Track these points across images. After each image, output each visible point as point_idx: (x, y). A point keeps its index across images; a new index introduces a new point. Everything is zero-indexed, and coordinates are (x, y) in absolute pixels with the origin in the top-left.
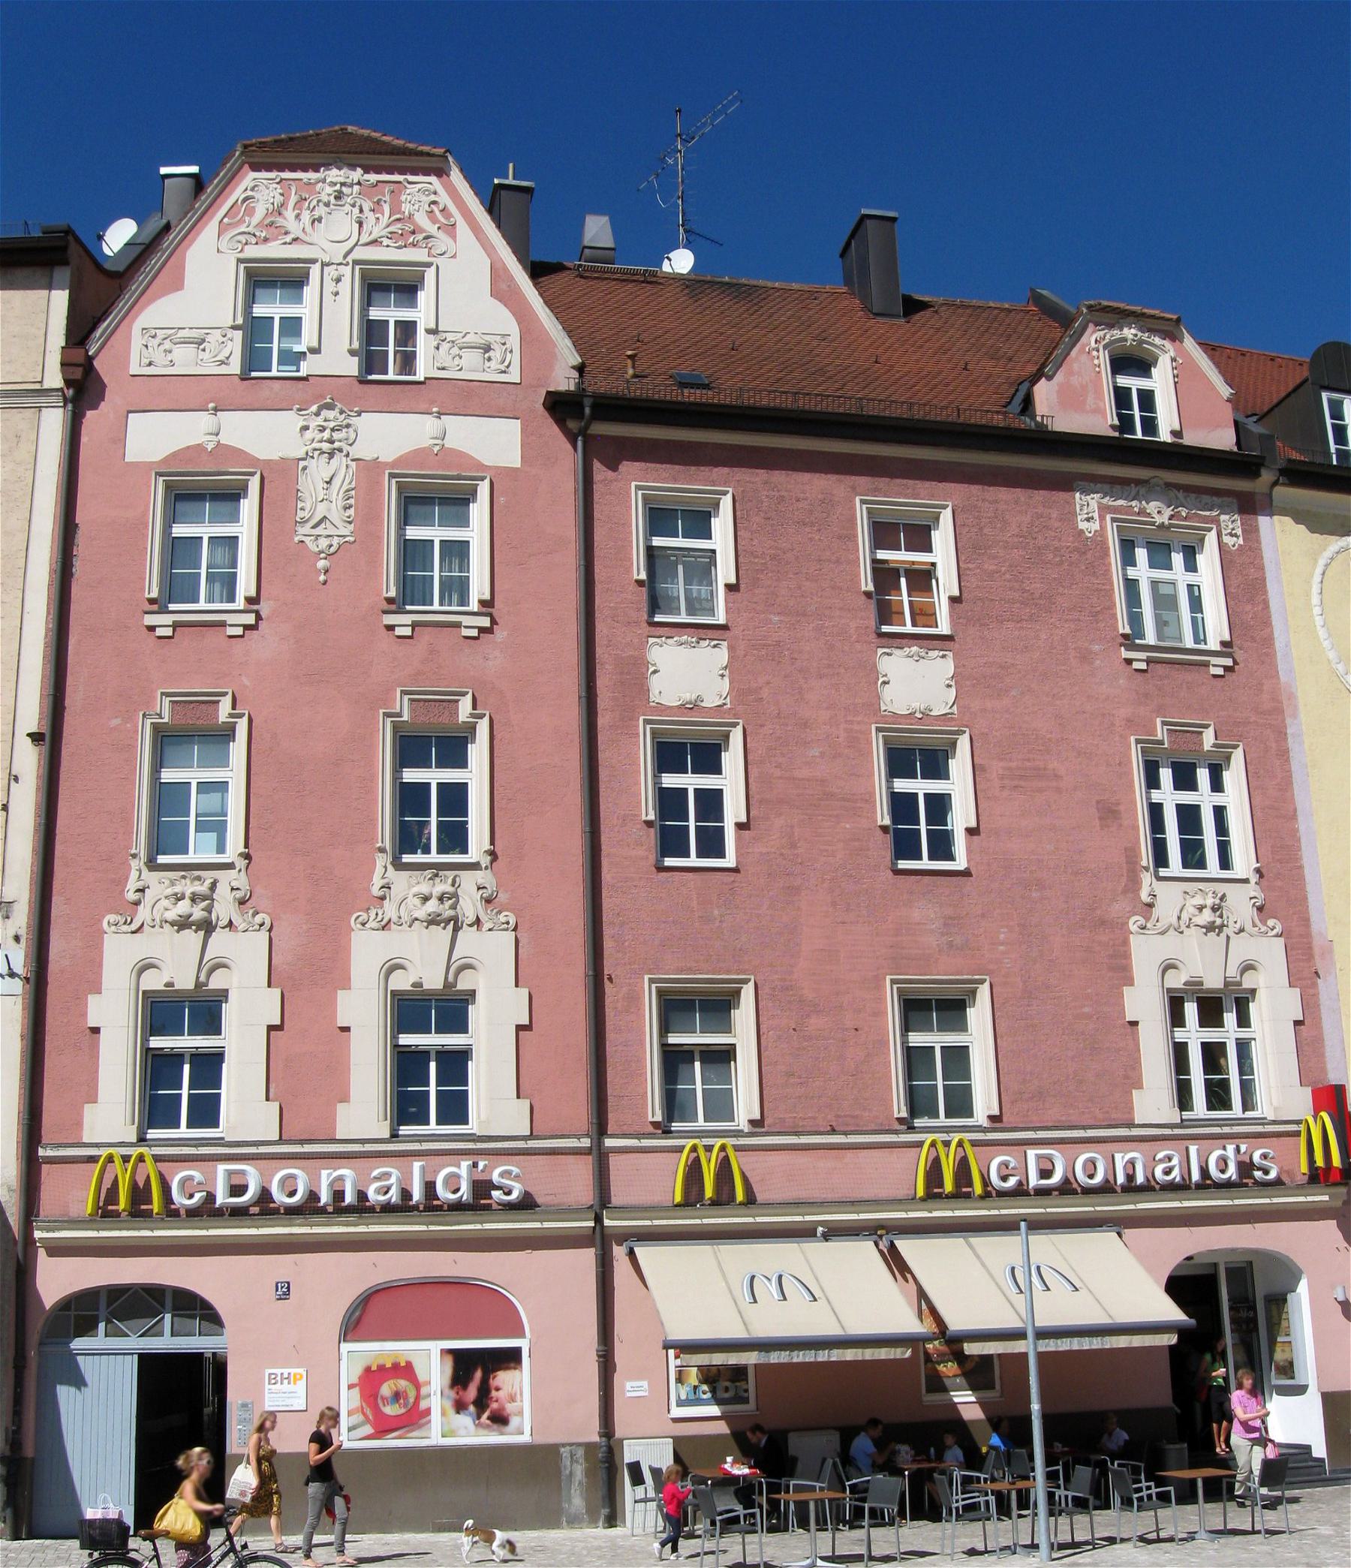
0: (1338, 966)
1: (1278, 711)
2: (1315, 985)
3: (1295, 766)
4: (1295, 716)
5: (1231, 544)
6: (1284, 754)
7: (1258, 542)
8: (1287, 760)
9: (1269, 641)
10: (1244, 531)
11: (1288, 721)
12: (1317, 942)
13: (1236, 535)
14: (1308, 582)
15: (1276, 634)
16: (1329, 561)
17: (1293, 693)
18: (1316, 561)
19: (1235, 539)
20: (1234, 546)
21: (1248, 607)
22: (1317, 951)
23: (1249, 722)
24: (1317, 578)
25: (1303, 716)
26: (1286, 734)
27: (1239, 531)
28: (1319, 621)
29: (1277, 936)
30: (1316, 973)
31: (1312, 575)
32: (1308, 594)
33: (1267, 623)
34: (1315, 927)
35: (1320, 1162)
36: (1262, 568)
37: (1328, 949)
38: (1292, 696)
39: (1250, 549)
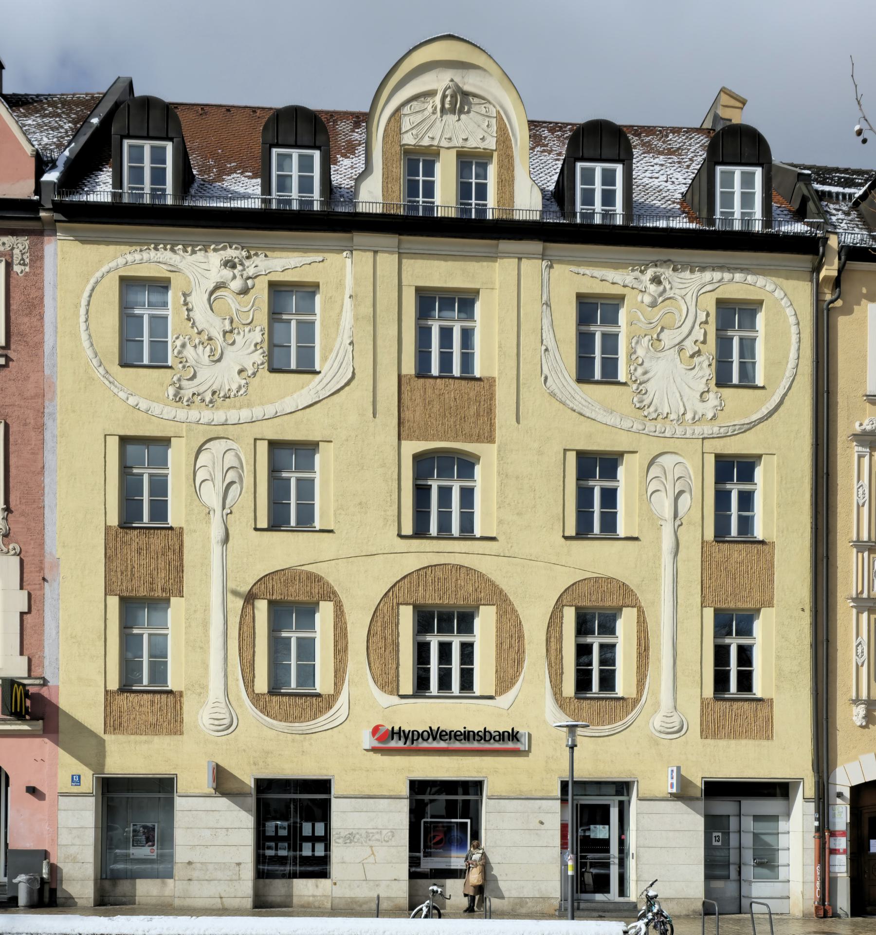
0: (62, 575)
1: (41, 395)
2: (42, 588)
3: (48, 435)
4: (52, 399)
5: (19, 272)
6: (40, 428)
7: (42, 267)
8: (42, 432)
9: (40, 344)
10: (31, 260)
11: (47, 403)
12: (48, 559)
13: (24, 265)
14: (79, 297)
15: (46, 338)
16: (99, 279)
17: (53, 383)
18: (88, 281)
19: (23, 268)
20: (22, 272)
21: (26, 320)
22: (47, 565)
23: (14, 405)
24: (86, 294)
25: (58, 400)
26: (43, 413)
27: (27, 261)
28: (83, 326)
29: (15, 554)
30: (44, 579)
31: (83, 292)
32: (77, 306)
33: (39, 330)
34: (47, 548)
35: (18, 710)
36: (41, 289)
37: (56, 565)
38: (52, 385)
39: (34, 274)
